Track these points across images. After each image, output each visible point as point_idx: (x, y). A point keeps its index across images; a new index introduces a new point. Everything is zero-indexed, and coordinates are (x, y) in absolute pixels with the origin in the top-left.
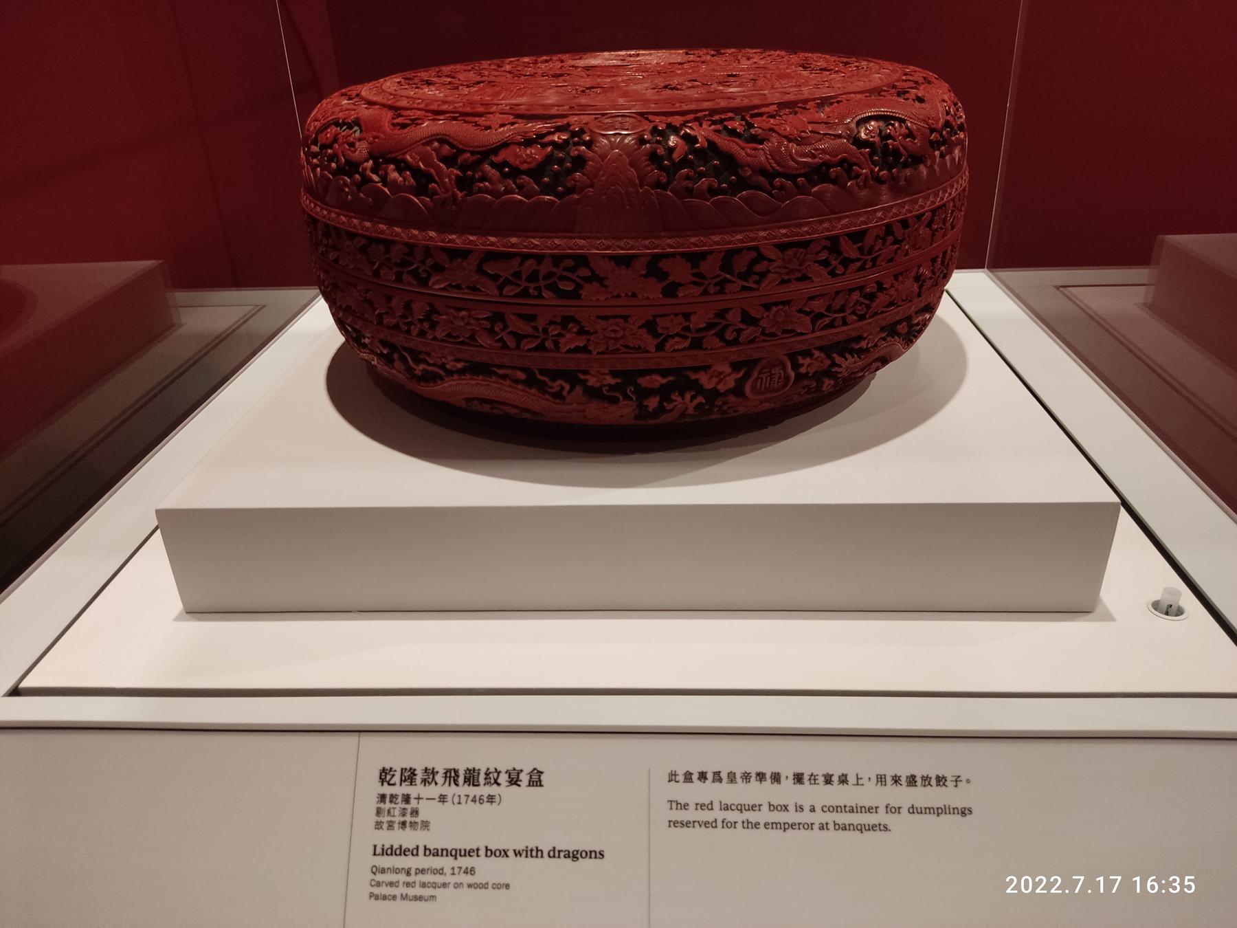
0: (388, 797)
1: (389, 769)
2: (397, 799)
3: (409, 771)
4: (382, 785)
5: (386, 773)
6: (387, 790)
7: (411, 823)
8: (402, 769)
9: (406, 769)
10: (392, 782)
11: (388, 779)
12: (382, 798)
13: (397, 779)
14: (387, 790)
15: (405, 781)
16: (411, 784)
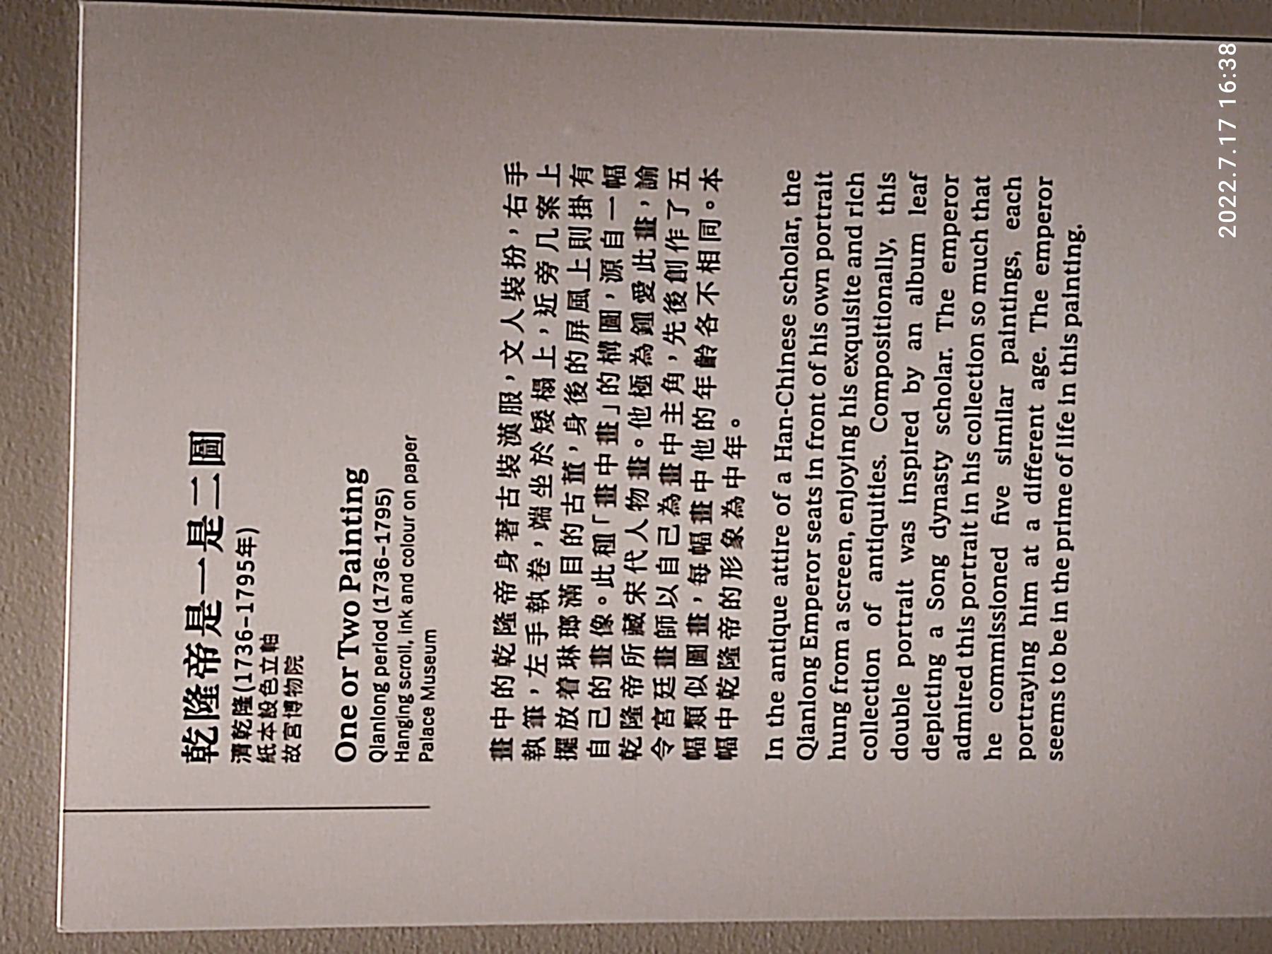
0: (237, 741)
1: (186, 744)
2: (241, 724)
3: (190, 702)
4: (216, 754)
5: (193, 749)
6: (224, 745)
7: (287, 694)
8: (186, 717)
9: (186, 709)
10: (211, 738)
11: (206, 745)
12: (238, 751)
13: (204, 726)
14: (224, 745)
15: (209, 710)
16: (216, 696)
